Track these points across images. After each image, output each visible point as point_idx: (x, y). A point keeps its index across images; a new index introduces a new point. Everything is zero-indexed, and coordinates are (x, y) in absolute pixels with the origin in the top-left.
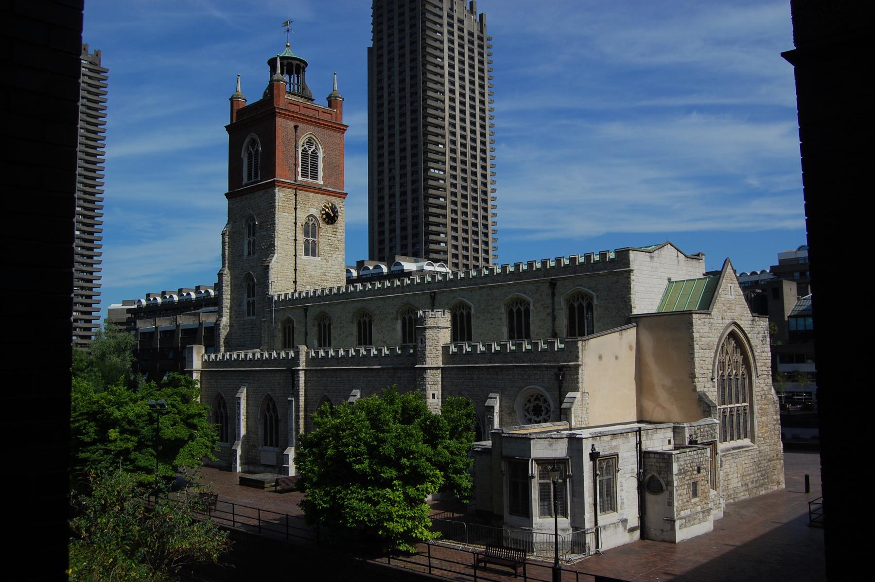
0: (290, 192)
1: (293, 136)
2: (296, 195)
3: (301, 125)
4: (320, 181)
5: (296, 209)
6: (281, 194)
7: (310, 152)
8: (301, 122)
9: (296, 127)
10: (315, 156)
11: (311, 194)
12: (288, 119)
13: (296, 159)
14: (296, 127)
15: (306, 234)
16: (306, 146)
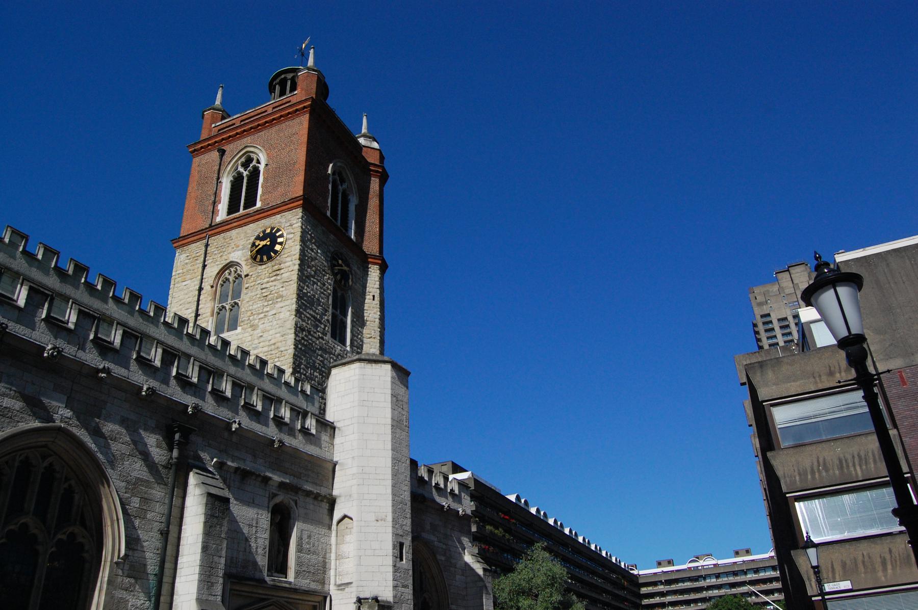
0: (197, 248)
1: (217, 168)
2: (207, 246)
3: (228, 148)
4: (259, 204)
5: (204, 266)
6: (183, 256)
7: (245, 173)
8: (230, 142)
9: (222, 152)
10: (255, 173)
11: (234, 233)
12: (210, 150)
13: (216, 194)
14: (222, 152)
15: (223, 298)
16: (241, 169)
